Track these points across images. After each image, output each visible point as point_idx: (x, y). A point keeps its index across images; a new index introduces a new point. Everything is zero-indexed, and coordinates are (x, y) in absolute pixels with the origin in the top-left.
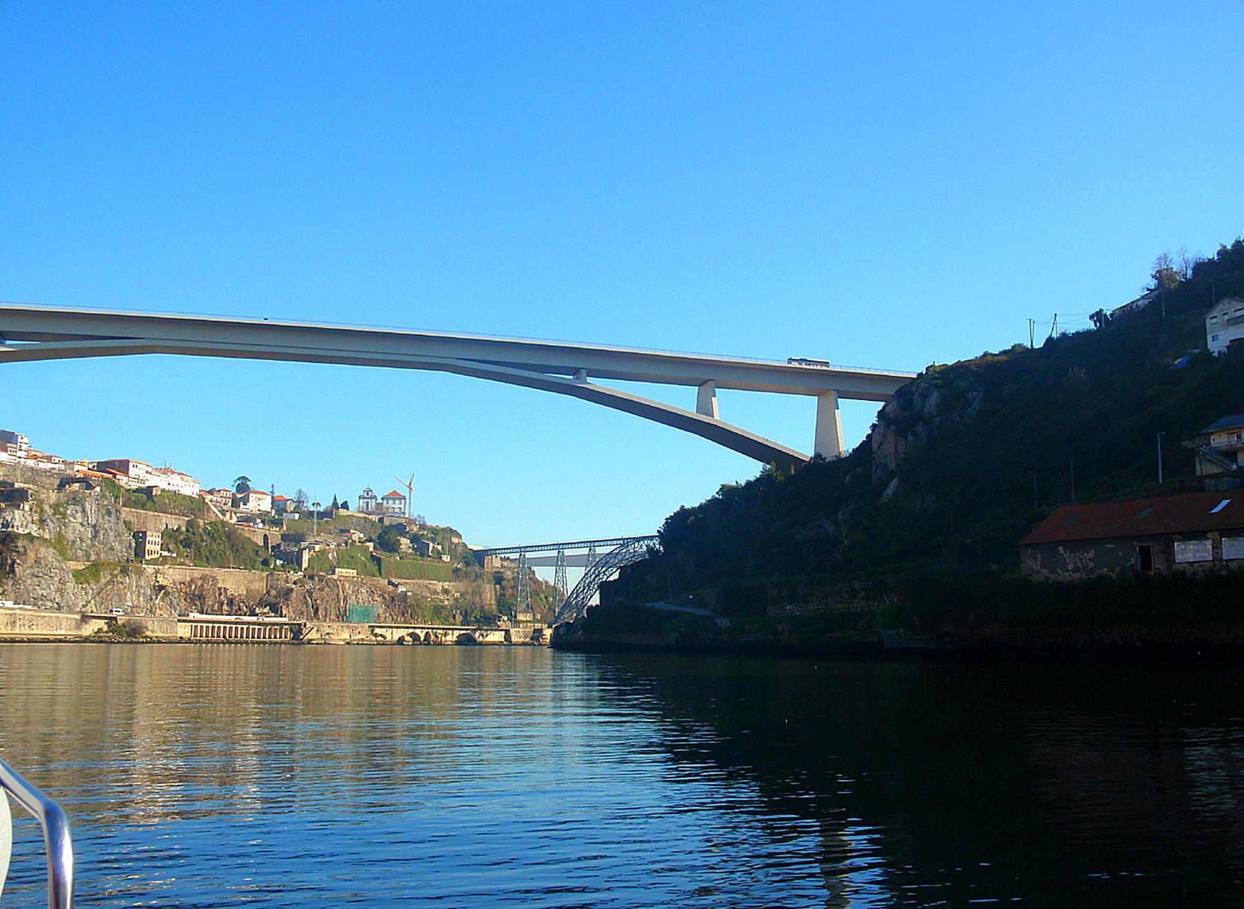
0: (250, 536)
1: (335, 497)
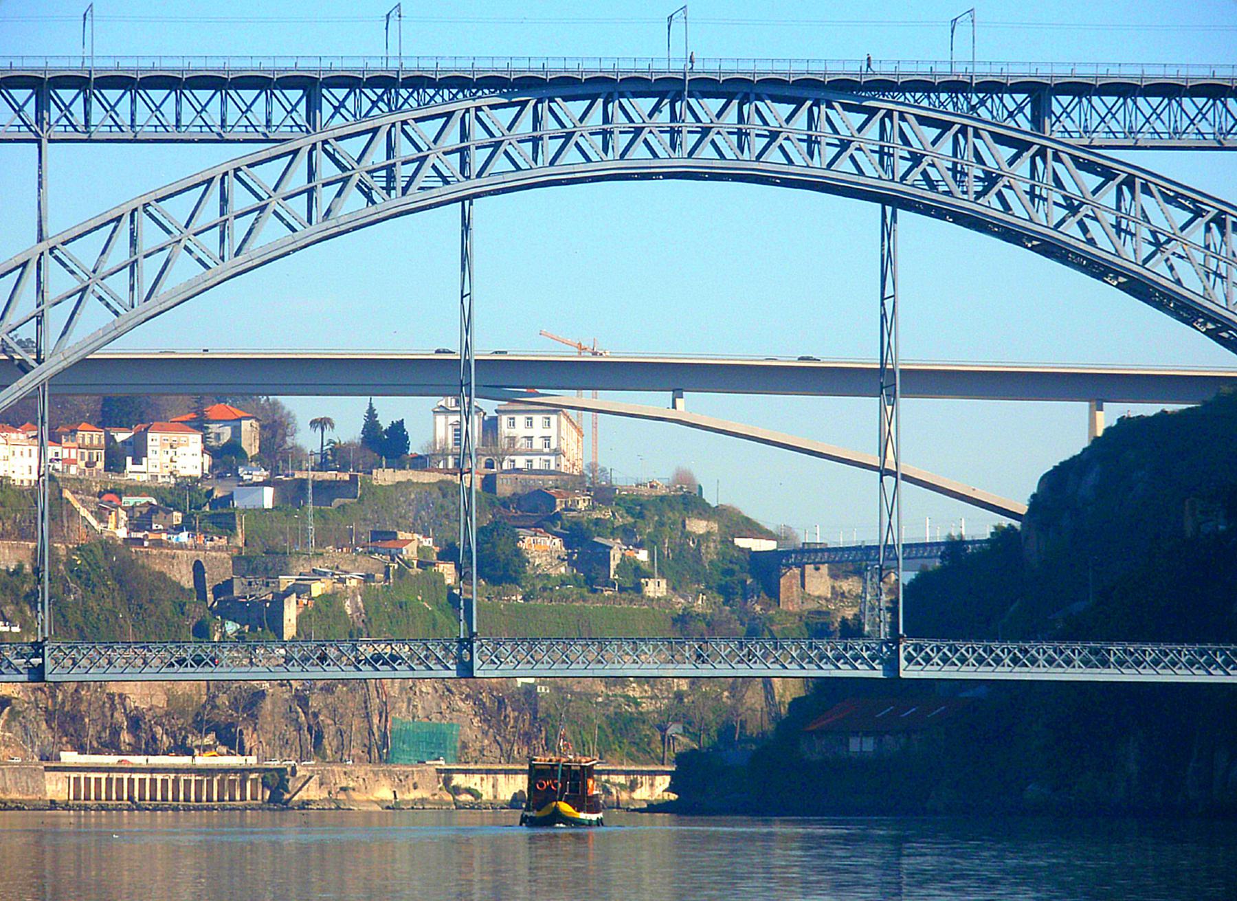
0: (164, 569)
1: (371, 404)
